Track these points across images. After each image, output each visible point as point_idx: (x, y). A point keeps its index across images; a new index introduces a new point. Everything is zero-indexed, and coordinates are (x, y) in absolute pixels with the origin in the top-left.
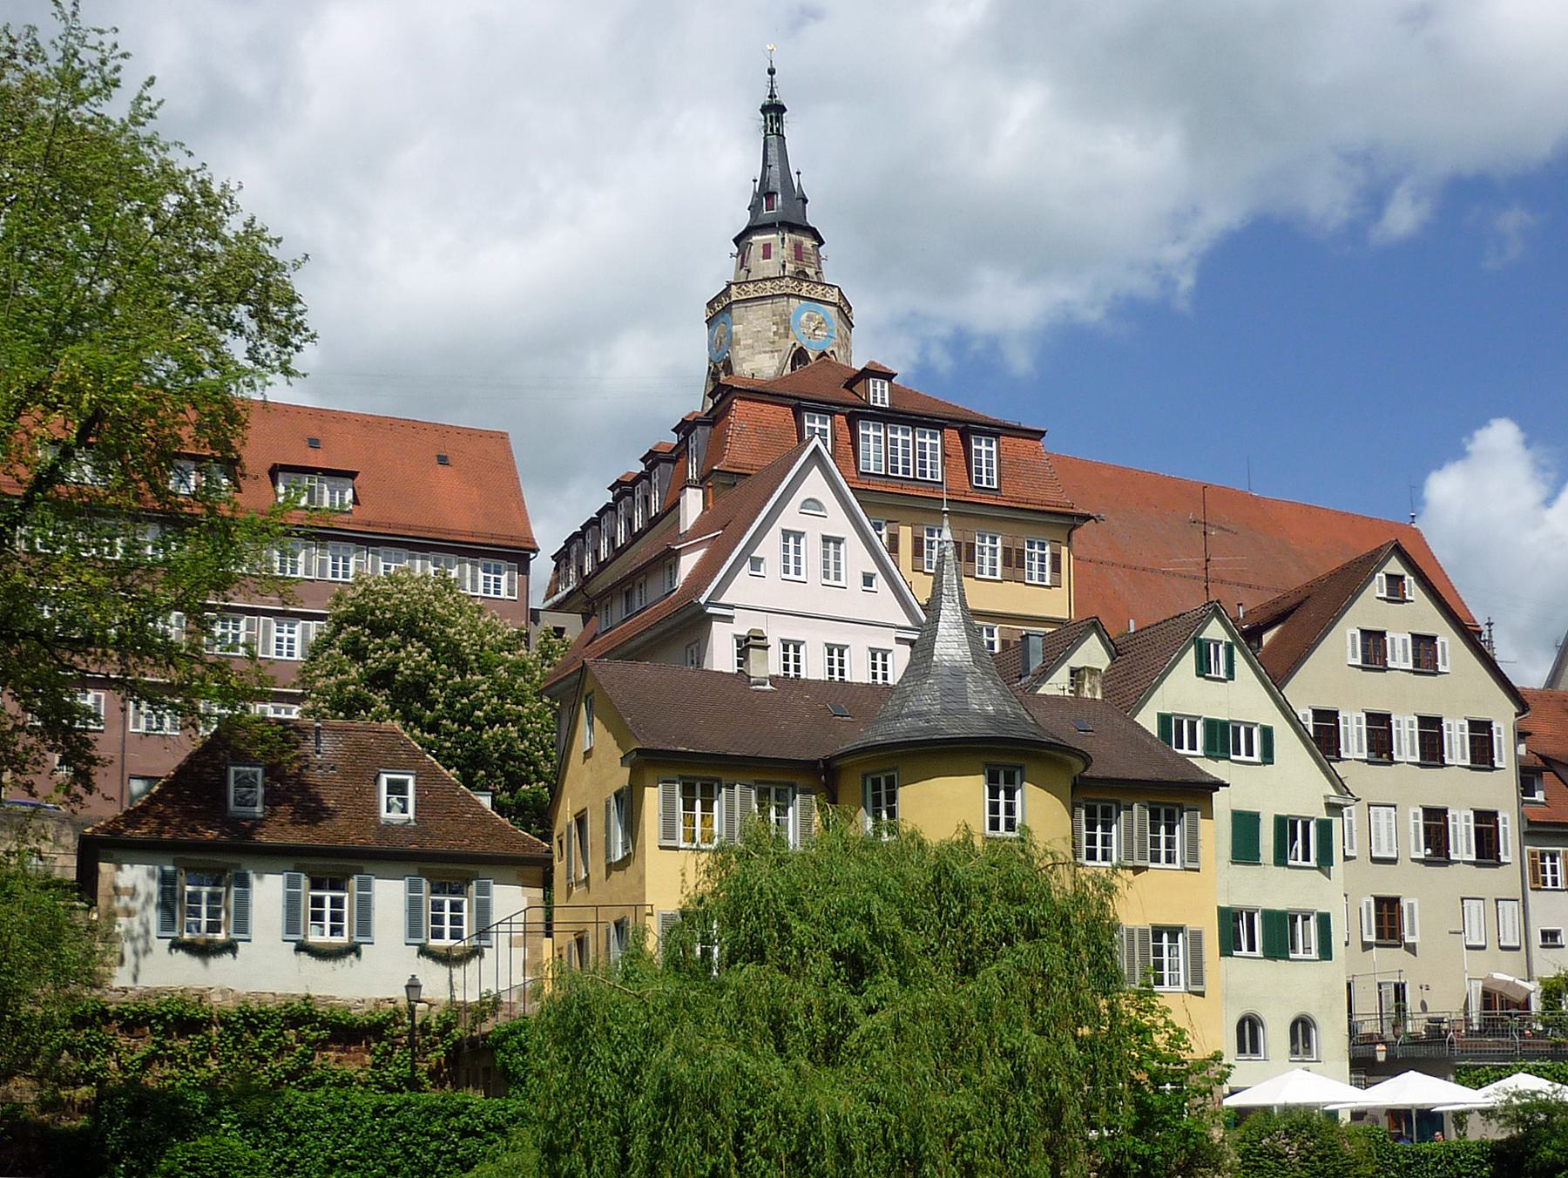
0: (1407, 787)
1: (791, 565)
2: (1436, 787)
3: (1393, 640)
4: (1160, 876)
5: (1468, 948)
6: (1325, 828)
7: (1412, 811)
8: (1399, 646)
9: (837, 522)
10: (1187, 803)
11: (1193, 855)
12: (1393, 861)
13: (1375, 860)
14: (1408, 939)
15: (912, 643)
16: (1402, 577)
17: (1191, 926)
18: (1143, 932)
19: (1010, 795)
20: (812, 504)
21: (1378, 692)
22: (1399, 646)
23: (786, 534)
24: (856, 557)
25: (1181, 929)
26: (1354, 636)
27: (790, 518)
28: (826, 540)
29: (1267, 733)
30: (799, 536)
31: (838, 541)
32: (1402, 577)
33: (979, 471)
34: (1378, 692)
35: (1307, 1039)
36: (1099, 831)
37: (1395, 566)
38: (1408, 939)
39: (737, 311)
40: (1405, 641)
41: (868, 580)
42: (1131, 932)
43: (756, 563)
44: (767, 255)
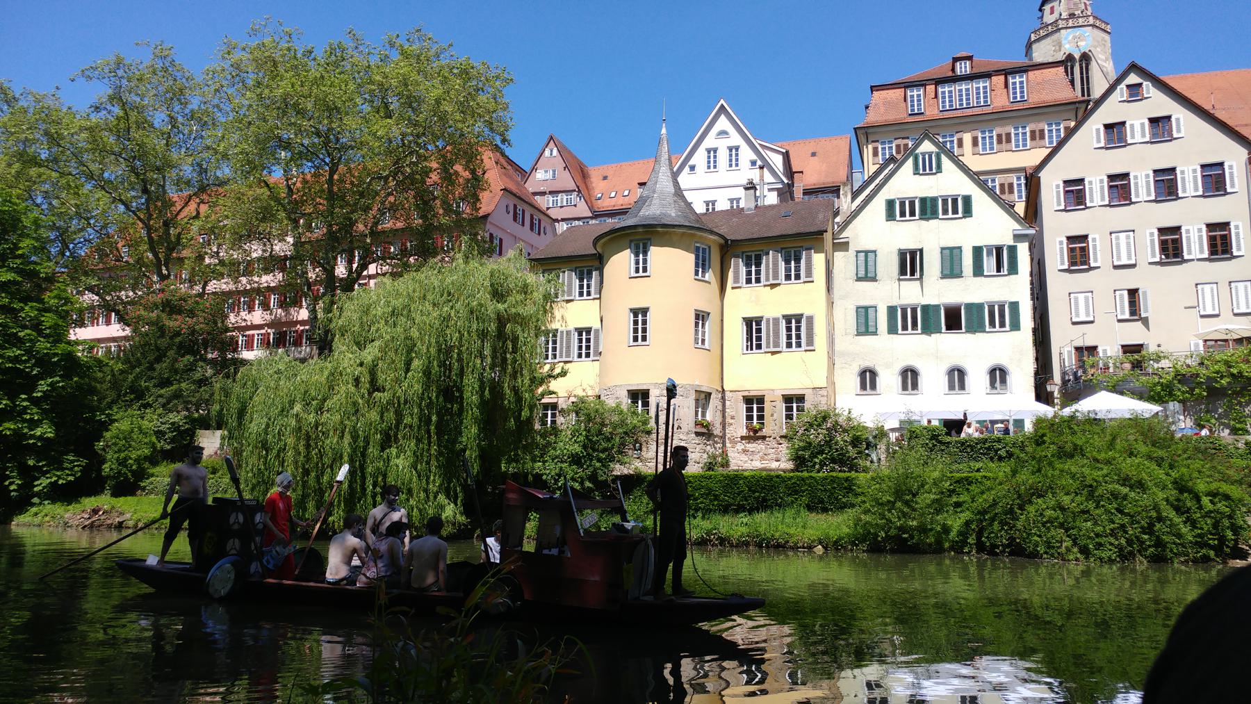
0: (1146, 217)
1: (712, 164)
2: (1168, 214)
3: (1132, 126)
5: (1202, 316)
6: (1013, 250)
7: (1148, 232)
8: (1137, 128)
9: (736, 139)
10: (806, 245)
11: (809, 273)
12: (1133, 266)
13: (1116, 267)
14: (1143, 315)
15: (777, 189)
16: (1140, 85)
17: (807, 313)
18: (776, 320)
19: (645, 253)
20: (723, 133)
21: (1117, 161)
22: (1137, 128)
23: (709, 151)
24: (746, 154)
25: (802, 315)
26: (1098, 130)
27: (710, 142)
28: (730, 149)
29: (967, 200)
30: (715, 150)
31: (737, 148)
32: (1140, 85)
33: (1015, 93)
34: (1117, 161)
35: (1003, 381)
36: (753, 268)
37: (1133, 79)
38: (1143, 315)
39: (1034, 46)
40: (1143, 125)
42: (768, 320)
43: (692, 168)
44: (1052, 13)
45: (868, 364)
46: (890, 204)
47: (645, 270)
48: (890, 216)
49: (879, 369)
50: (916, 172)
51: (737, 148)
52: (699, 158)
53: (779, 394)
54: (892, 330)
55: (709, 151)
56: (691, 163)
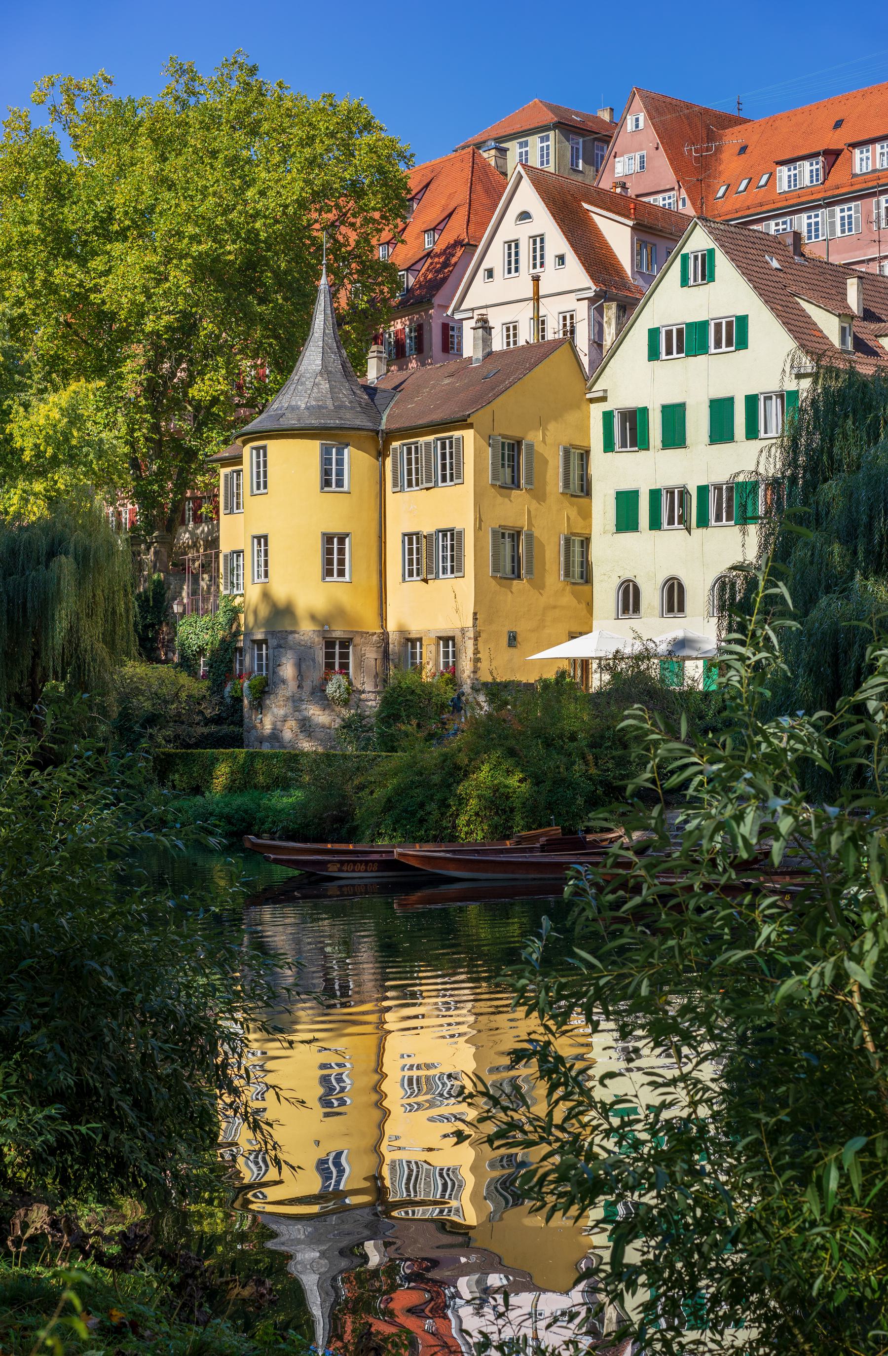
4: (445, 493)
17: (458, 527)
28: (534, 238)
29: (743, 321)
30: (517, 243)
41: (561, 259)
43: (490, 273)
45: (628, 575)
46: (653, 334)
47: (265, 487)
48: (653, 355)
49: (640, 582)
50: (684, 282)
51: (542, 238)
52: (495, 257)
53: (433, 635)
54: (655, 524)
55: (509, 243)
56: (485, 265)
